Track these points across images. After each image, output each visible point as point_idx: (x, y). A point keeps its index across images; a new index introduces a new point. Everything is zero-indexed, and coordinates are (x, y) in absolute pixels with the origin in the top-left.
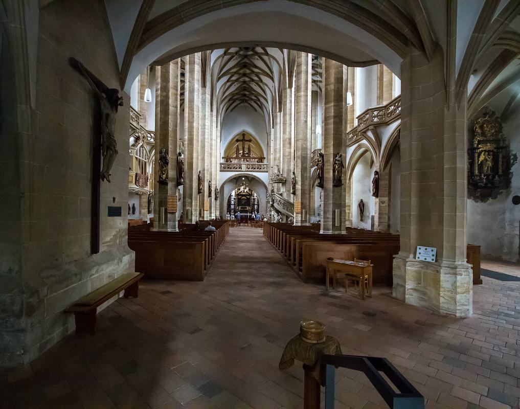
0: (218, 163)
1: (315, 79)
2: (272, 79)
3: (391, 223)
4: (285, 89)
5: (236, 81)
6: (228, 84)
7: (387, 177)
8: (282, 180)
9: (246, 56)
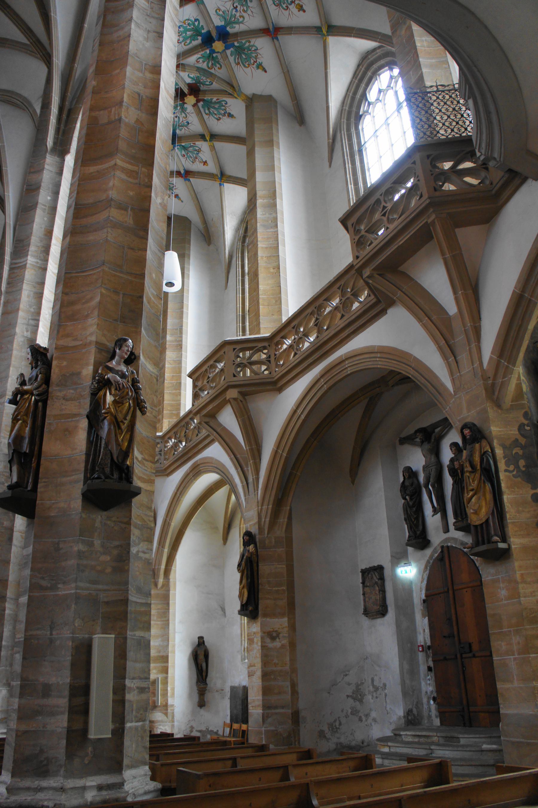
3: (301, 705)
7: (281, 550)
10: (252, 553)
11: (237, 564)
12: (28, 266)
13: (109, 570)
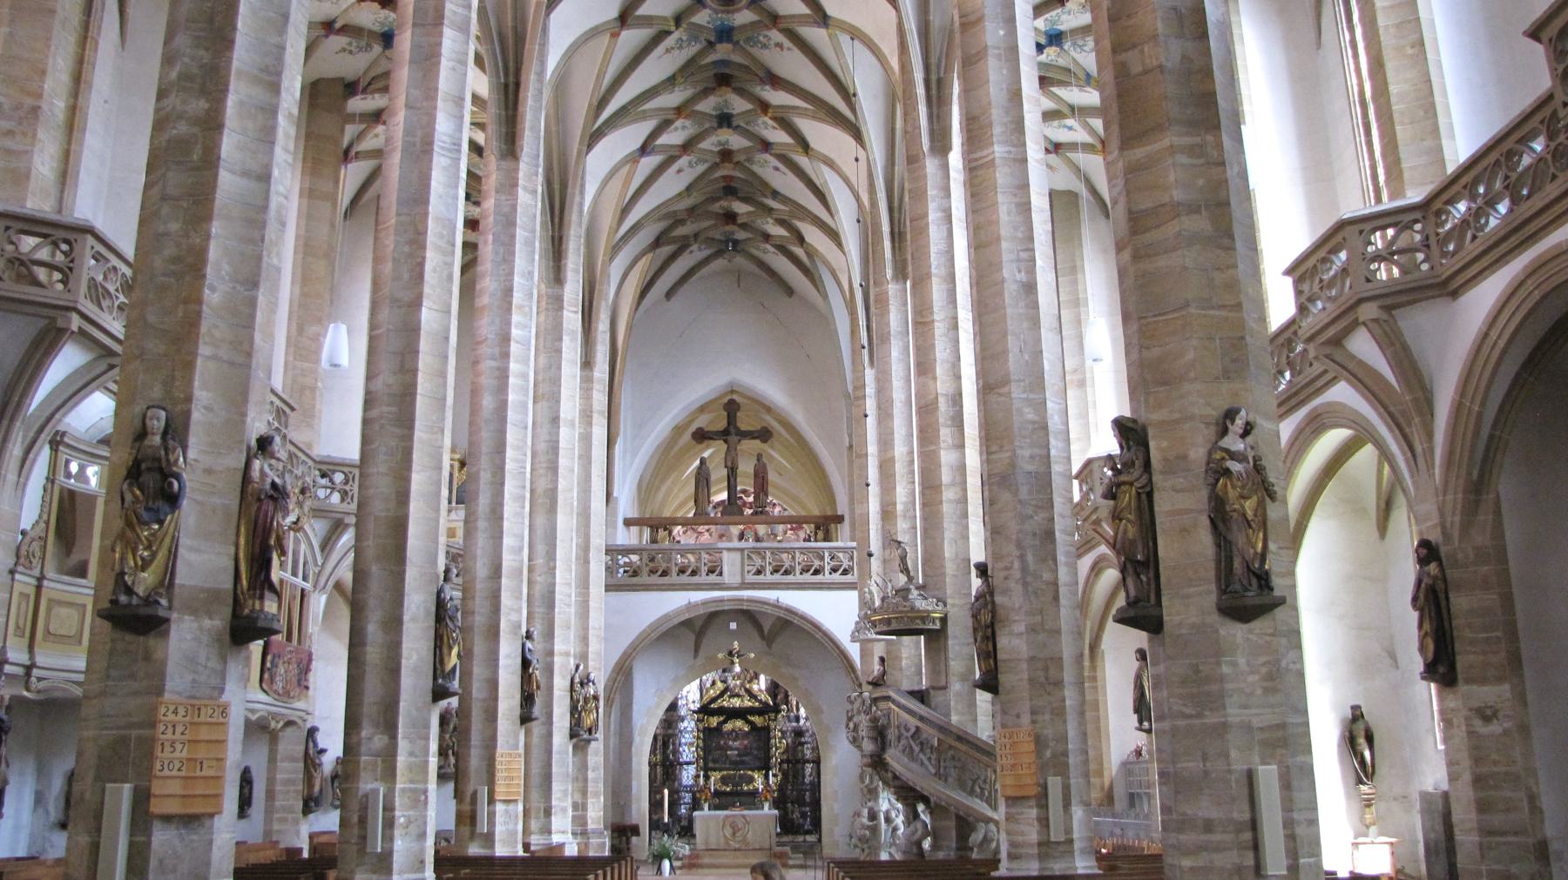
0: (598, 541)
1: (1062, 136)
2: (857, 134)
4: (913, 160)
5: (687, 147)
6: (649, 163)
8: (925, 617)
9: (725, 34)
10: (1435, 578)
11: (1409, 597)
12: (997, 161)
13: (1259, 691)
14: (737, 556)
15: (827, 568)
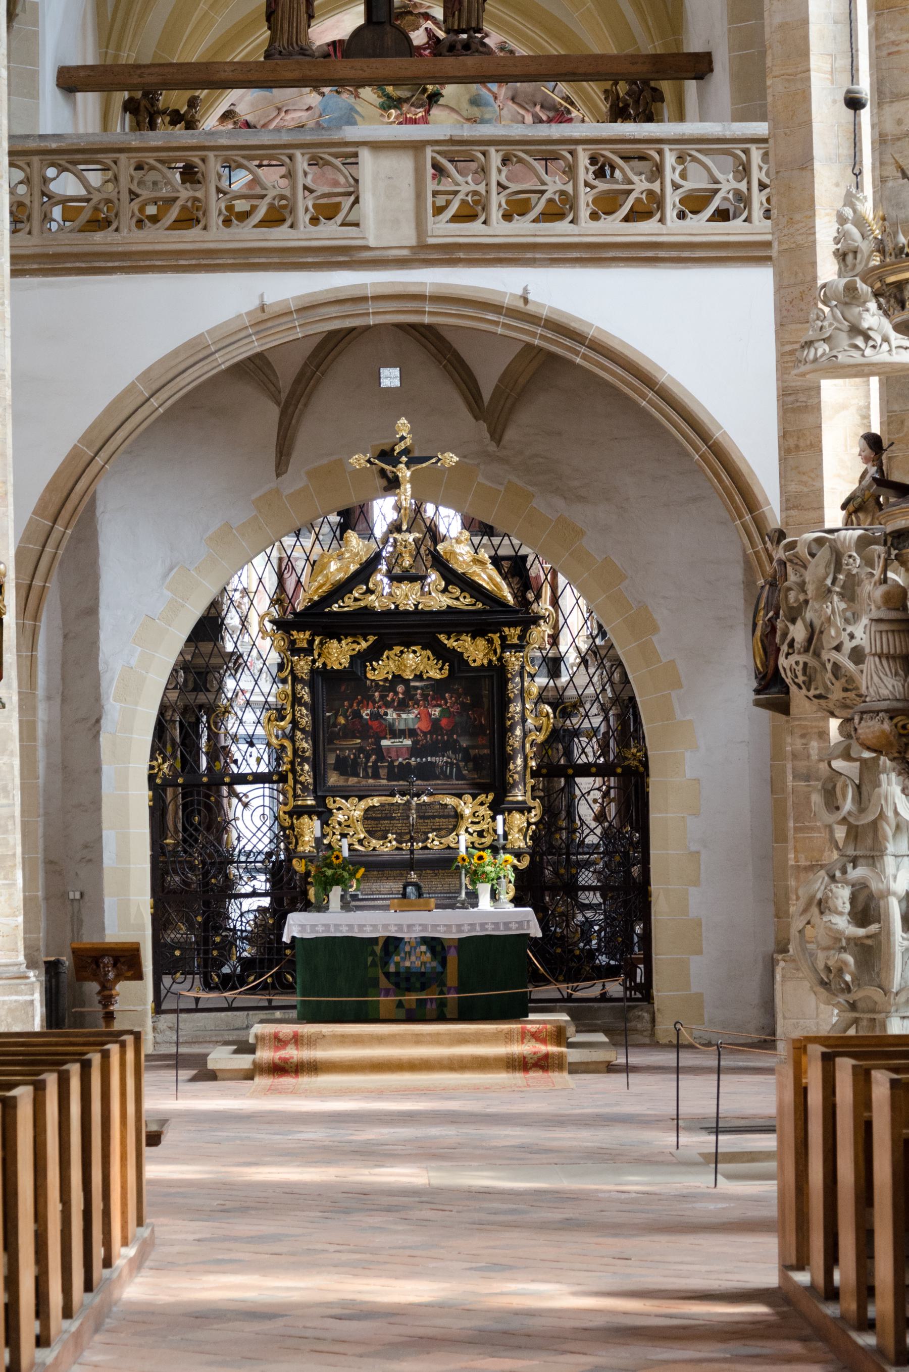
14: (404, 164)
15: (672, 199)
